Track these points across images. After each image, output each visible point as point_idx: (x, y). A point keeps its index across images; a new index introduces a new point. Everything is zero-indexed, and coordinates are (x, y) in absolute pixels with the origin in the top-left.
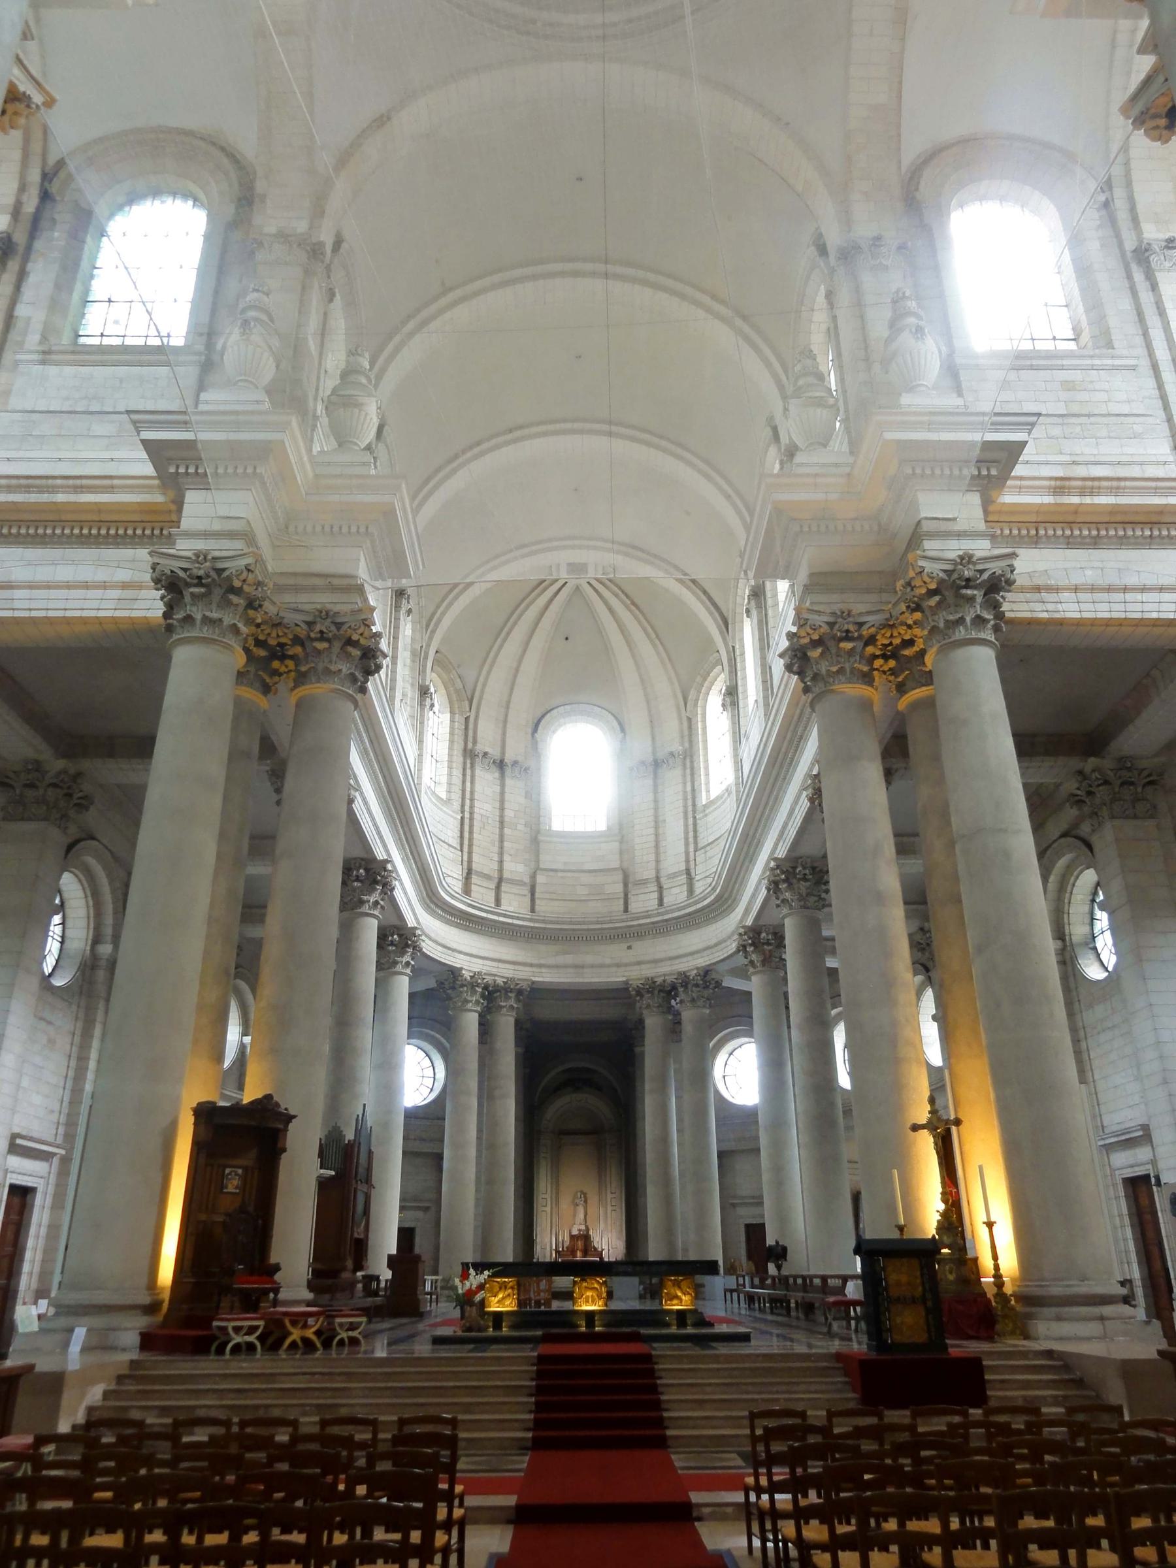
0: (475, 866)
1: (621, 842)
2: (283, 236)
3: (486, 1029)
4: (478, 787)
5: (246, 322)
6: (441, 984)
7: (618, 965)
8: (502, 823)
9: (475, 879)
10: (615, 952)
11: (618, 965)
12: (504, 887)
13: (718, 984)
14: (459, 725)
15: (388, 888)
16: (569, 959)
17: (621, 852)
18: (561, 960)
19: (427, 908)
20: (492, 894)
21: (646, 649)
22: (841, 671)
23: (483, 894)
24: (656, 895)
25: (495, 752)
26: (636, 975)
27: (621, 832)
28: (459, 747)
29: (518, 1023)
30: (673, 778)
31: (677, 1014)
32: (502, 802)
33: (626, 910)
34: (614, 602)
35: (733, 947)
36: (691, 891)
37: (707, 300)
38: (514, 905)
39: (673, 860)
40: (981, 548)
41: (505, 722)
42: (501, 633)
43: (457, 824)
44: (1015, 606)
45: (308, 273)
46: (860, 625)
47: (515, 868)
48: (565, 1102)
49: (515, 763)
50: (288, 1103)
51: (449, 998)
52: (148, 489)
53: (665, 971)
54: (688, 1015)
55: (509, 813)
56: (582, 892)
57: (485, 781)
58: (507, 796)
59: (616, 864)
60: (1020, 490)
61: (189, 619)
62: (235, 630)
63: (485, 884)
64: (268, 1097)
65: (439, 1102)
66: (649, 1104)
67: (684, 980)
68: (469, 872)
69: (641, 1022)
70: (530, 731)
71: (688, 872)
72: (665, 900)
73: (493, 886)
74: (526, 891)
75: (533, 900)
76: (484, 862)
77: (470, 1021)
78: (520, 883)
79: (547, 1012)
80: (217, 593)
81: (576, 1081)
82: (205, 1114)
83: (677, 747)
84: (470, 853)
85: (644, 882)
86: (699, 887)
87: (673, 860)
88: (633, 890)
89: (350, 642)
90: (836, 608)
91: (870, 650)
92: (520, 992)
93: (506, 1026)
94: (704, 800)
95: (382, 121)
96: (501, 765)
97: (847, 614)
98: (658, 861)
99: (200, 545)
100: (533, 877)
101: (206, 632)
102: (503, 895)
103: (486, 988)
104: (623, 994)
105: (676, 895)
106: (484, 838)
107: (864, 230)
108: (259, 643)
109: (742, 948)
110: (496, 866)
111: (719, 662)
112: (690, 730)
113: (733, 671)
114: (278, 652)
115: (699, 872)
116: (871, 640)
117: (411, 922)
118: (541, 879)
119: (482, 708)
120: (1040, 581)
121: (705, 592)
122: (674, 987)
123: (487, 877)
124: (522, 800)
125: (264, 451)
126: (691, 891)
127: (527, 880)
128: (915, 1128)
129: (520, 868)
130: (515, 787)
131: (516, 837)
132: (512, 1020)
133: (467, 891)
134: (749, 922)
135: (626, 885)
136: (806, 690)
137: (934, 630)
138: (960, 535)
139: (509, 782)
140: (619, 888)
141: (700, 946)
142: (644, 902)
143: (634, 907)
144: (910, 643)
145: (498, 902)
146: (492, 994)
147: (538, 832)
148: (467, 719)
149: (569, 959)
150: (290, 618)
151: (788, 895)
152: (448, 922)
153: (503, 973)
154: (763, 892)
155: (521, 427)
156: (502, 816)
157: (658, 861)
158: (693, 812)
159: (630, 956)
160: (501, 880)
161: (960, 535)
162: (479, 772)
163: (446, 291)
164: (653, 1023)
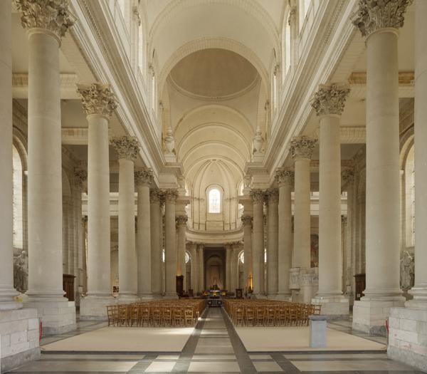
3: (197, 251)
10: (221, 237)
21: (228, 174)
23: (196, 227)
26: (224, 242)
27: (223, 213)
29: (204, 251)
47: (202, 221)
48: (212, 259)
53: (230, 241)
54: (234, 250)
59: (221, 219)
67: (234, 243)
68: (193, 223)
71: (236, 223)
76: (196, 221)
86: (237, 227)
87: (233, 221)
93: (201, 251)
96: (199, 199)
104: (223, 244)
105: (233, 228)
130: (202, 204)
131: (203, 214)
133: (193, 227)
140: (222, 225)
142: (227, 228)
146: (198, 246)
164: (228, 251)
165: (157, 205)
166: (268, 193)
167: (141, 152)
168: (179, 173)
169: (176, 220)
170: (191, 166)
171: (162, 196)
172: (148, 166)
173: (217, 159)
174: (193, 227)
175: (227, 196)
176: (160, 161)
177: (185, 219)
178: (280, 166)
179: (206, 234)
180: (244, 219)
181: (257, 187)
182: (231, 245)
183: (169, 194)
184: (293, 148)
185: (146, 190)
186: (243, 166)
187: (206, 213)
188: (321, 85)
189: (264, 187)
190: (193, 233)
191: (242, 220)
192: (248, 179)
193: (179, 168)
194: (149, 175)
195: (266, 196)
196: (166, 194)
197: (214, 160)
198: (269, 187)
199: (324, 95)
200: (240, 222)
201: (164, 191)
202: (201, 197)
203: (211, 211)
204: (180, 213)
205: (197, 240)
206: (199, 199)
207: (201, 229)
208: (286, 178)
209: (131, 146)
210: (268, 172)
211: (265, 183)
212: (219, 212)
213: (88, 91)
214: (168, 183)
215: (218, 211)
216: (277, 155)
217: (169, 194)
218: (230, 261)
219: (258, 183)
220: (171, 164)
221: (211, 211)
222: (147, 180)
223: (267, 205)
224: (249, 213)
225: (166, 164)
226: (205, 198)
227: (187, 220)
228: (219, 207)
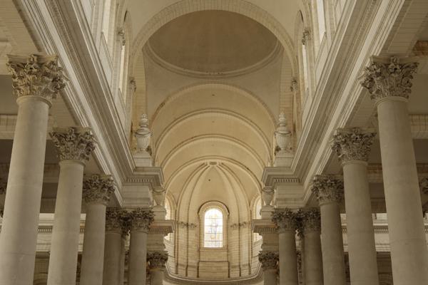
0: (179, 262)
1: (228, 252)
4: (180, 234)
9: (179, 267)
12: (189, 269)
17: (228, 255)
23: (182, 272)
25: (185, 221)
27: (227, 248)
32: (188, 238)
33: (229, 277)
34: (226, 172)
36: (250, 274)
39: (245, 261)
41: (188, 209)
43: (173, 248)
46: (273, 254)
47: (193, 262)
49: (192, 224)
55: (190, 242)
56: (214, 269)
58: (190, 237)
63: (182, 268)
68: (177, 264)
70: (197, 211)
73: (185, 268)
75: (198, 272)
76: (182, 261)
83: (246, 220)
84: (178, 258)
85: (235, 267)
86: (252, 272)
87: (245, 261)
88: (231, 269)
89: (162, 258)
95: (162, 105)
96: (187, 225)
98: (239, 259)
100: (198, 263)
102: (188, 272)
105: (245, 273)
106: (182, 253)
110: (185, 261)
111: (258, 194)
115: (253, 265)
118: (201, 265)
119: (181, 206)
121: (255, 176)
124: (194, 237)
127: (196, 265)
129: (194, 261)
130: (192, 233)
131: (193, 248)
135: (229, 267)
139: (190, 231)
140: (227, 268)
143: (231, 275)
145: (187, 275)
147: (200, 248)
148: (176, 211)
155: (196, 137)
156: (188, 243)
157: (239, 259)
160: (187, 266)
162: (180, 229)
165: (116, 234)
166: (302, 215)
167: (97, 152)
168: (155, 182)
169: (148, 260)
170: (177, 171)
171: (126, 219)
172: (107, 172)
173: (218, 161)
175: (234, 219)
176: (127, 164)
177: (164, 258)
178: (319, 172)
180: (263, 258)
181: (284, 206)
183: (138, 216)
184: (339, 145)
185: (101, 209)
186: (259, 171)
187: (200, 249)
188: (374, 57)
189: (296, 206)
191: (260, 260)
192: (269, 193)
193: (157, 175)
194: (106, 186)
195: (300, 219)
197: (213, 163)
198: (302, 206)
199: (378, 71)
200: (256, 264)
201: (130, 211)
202: (190, 222)
203: (207, 244)
204: (155, 248)
207: (189, 276)
208: (330, 192)
209: (82, 141)
210: (300, 181)
212: (221, 246)
213: (24, 64)
214: (136, 199)
216: (313, 156)
217: (138, 216)
219: (286, 200)
220: (143, 169)
221: (207, 244)
222: (103, 195)
223: (301, 234)
224: (273, 249)
225: (136, 169)
226: (198, 224)
227: (166, 260)
228: (221, 238)
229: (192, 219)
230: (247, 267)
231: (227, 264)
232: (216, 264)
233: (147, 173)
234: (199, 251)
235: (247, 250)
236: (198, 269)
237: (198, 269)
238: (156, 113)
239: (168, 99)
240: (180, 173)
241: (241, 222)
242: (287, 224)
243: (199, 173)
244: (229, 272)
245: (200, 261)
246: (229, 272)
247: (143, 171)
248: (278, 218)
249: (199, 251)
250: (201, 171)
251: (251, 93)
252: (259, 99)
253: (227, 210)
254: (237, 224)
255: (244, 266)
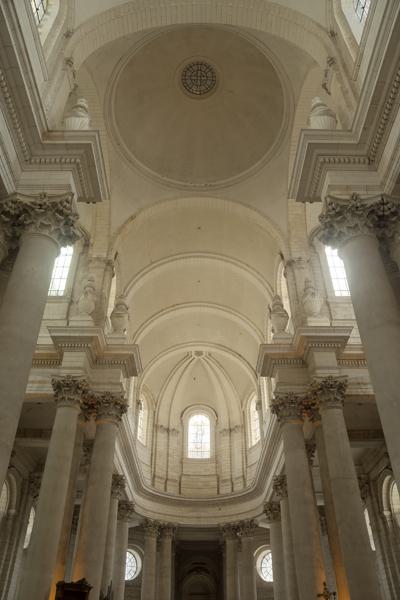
2: (98, 259)
3: (159, 545)
5: (86, 293)
6: (142, 525)
7: (215, 517)
8: (168, 454)
11: (215, 517)
13: (257, 526)
14: (151, 415)
15: (123, 486)
16: (195, 514)
18: (191, 514)
19: (139, 495)
20: (163, 486)
21: (226, 383)
22: (290, 415)
23: (160, 486)
24: (230, 487)
25: (165, 425)
26: (222, 521)
27: (216, 458)
28: (151, 423)
29: (173, 542)
30: (237, 437)
31: (240, 539)
32: (168, 446)
33: (218, 493)
35: (262, 510)
36: (245, 485)
37: (245, 266)
38: (172, 490)
40: (335, 373)
42: (169, 377)
44: (348, 392)
45: (106, 270)
47: (174, 474)
49: (174, 430)
50: (90, 582)
51: (144, 531)
52: (49, 349)
53: (235, 520)
55: (170, 452)
56: (200, 484)
57: (162, 437)
60: (351, 349)
61: (63, 398)
62: (79, 402)
64: (84, 579)
65: (139, 578)
66: (228, 581)
68: (154, 476)
69: (225, 542)
72: (235, 489)
74: (177, 484)
76: (160, 472)
77: (153, 541)
78: (175, 481)
79: (185, 537)
80: (73, 389)
81: (199, 568)
82: (61, 586)
83: (239, 423)
85: (225, 481)
86: (248, 484)
87: (238, 473)
89: (116, 404)
90: (288, 391)
91: (301, 407)
92: (174, 529)
93: (168, 542)
94: (249, 446)
96: (168, 430)
97: (291, 394)
99: (68, 371)
101: (69, 403)
103: (160, 527)
105: (239, 487)
106: (161, 462)
107: (295, 255)
108: (86, 404)
109: (265, 511)
111: (254, 390)
112: (244, 416)
113: (260, 394)
114: (91, 407)
116: (301, 403)
117: (131, 499)
120: (360, 381)
122: (238, 527)
123: (161, 478)
125: (91, 338)
126: (245, 485)
128: (319, 596)
129: (175, 474)
130: (174, 440)
131: (174, 461)
132: (170, 541)
133: (153, 485)
134: (268, 500)
136: (279, 421)
137: (321, 402)
138: (328, 368)
139: (171, 438)
141: (249, 509)
142: (226, 490)
143: (221, 492)
144: (314, 404)
145: (166, 489)
146: (163, 529)
147: (182, 459)
149: (195, 514)
150: (96, 395)
151: (281, 491)
152: (144, 498)
153: (169, 519)
154: (272, 490)
158: (246, 451)
159: (220, 513)
160: (167, 480)
161: (328, 368)
163: (153, 263)
164: (230, 543)
174: (153, 485)
175: (224, 423)
179: (179, 503)
182: (235, 529)
186: (253, 356)
187: (183, 460)
190: (153, 497)
193: (132, 357)
196: (26, 210)
197: (199, 353)
202: (171, 428)
205: (156, 517)
206: (168, 430)
210: (372, 160)
211: (367, 188)
212: (207, 455)
215: (207, 455)
218: (235, 568)
219: (348, 188)
229: (174, 423)
230: (241, 480)
231: (215, 478)
232: (202, 479)
233: (69, 142)
234: (181, 463)
235: (240, 457)
236: (180, 485)
237: (180, 485)
238: (123, 226)
239: (140, 212)
240: (159, 362)
241: (232, 427)
242: (356, 221)
243: (187, 363)
244: (218, 488)
245: (182, 474)
246: (218, 488)
247: (63, 138)
248: (339, 214)
249: (181, 463)
250: (187, 363)
251: (249, 206)
252: (259, 212)
253: (215, 416)
254: (227, 428)
255: (236, 479)
